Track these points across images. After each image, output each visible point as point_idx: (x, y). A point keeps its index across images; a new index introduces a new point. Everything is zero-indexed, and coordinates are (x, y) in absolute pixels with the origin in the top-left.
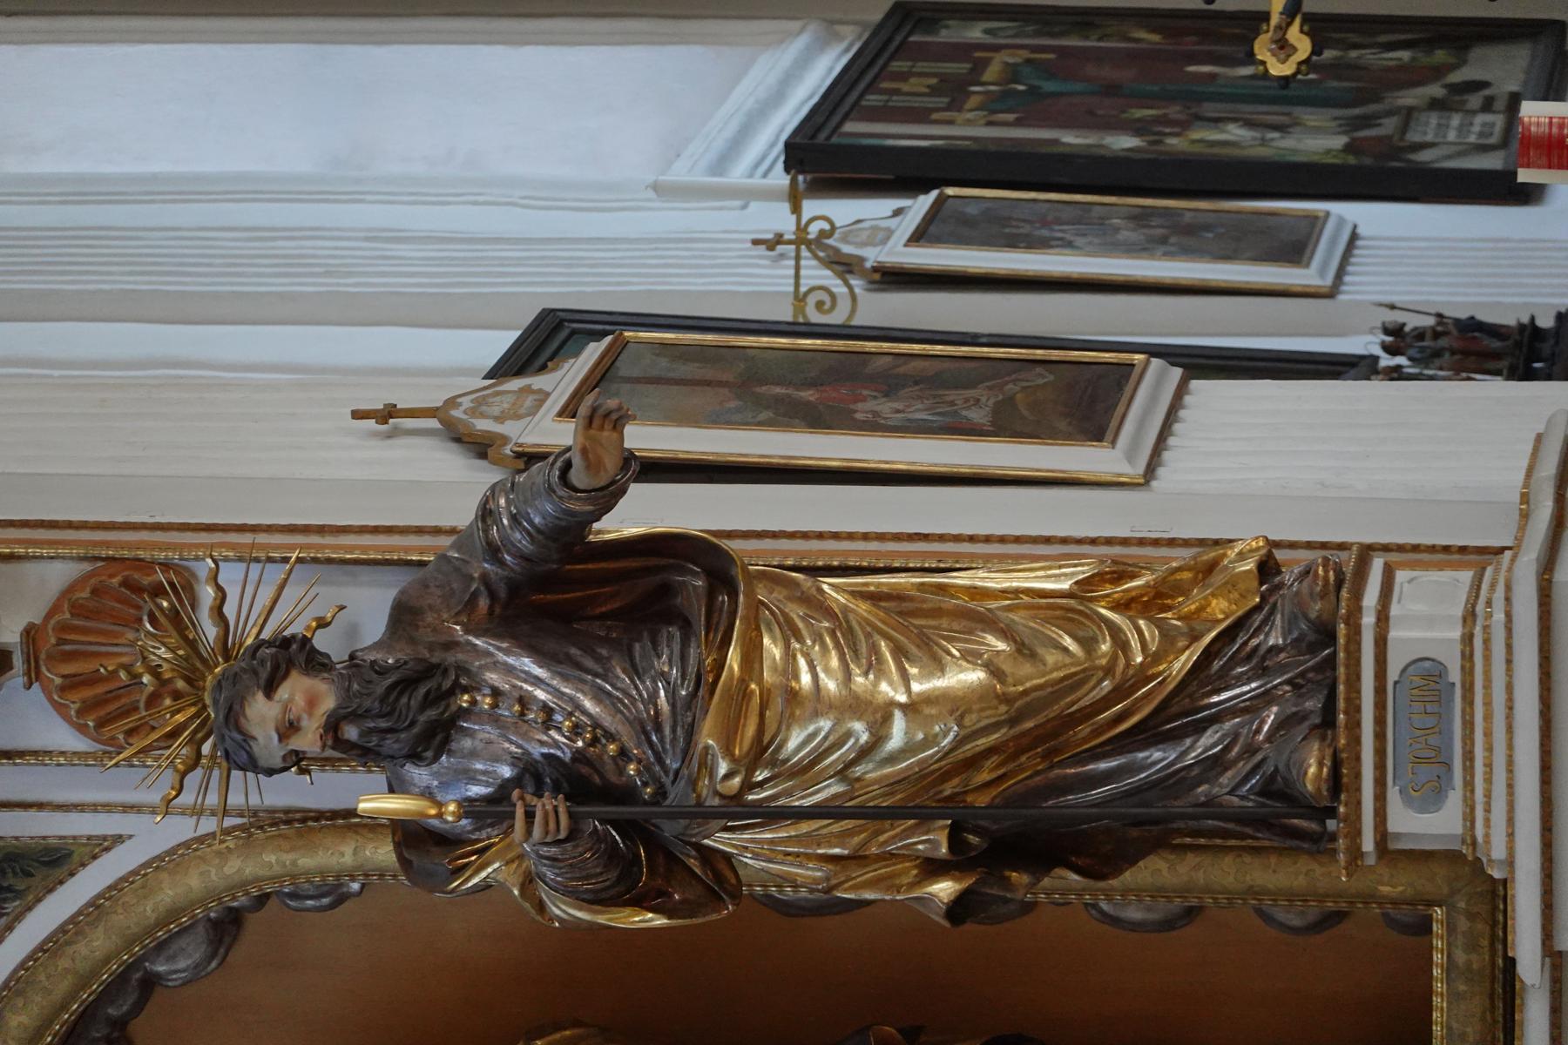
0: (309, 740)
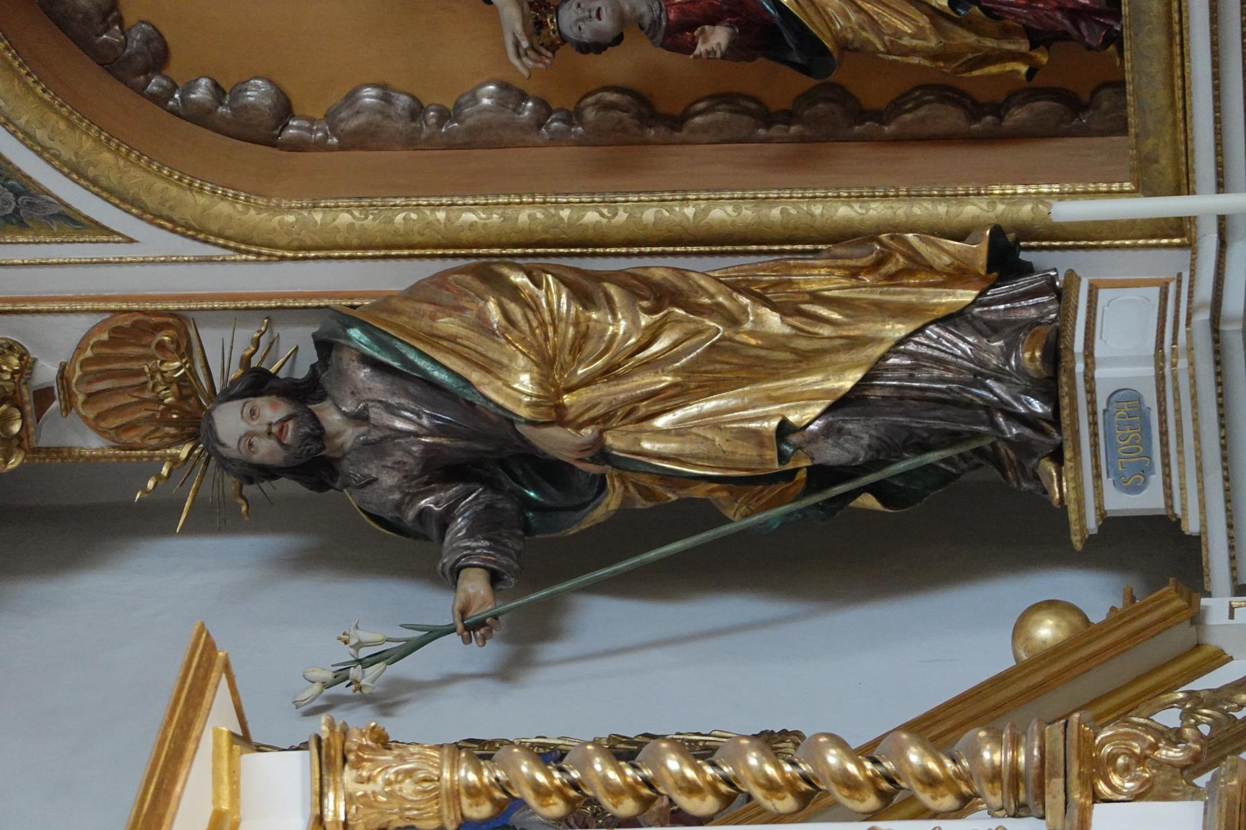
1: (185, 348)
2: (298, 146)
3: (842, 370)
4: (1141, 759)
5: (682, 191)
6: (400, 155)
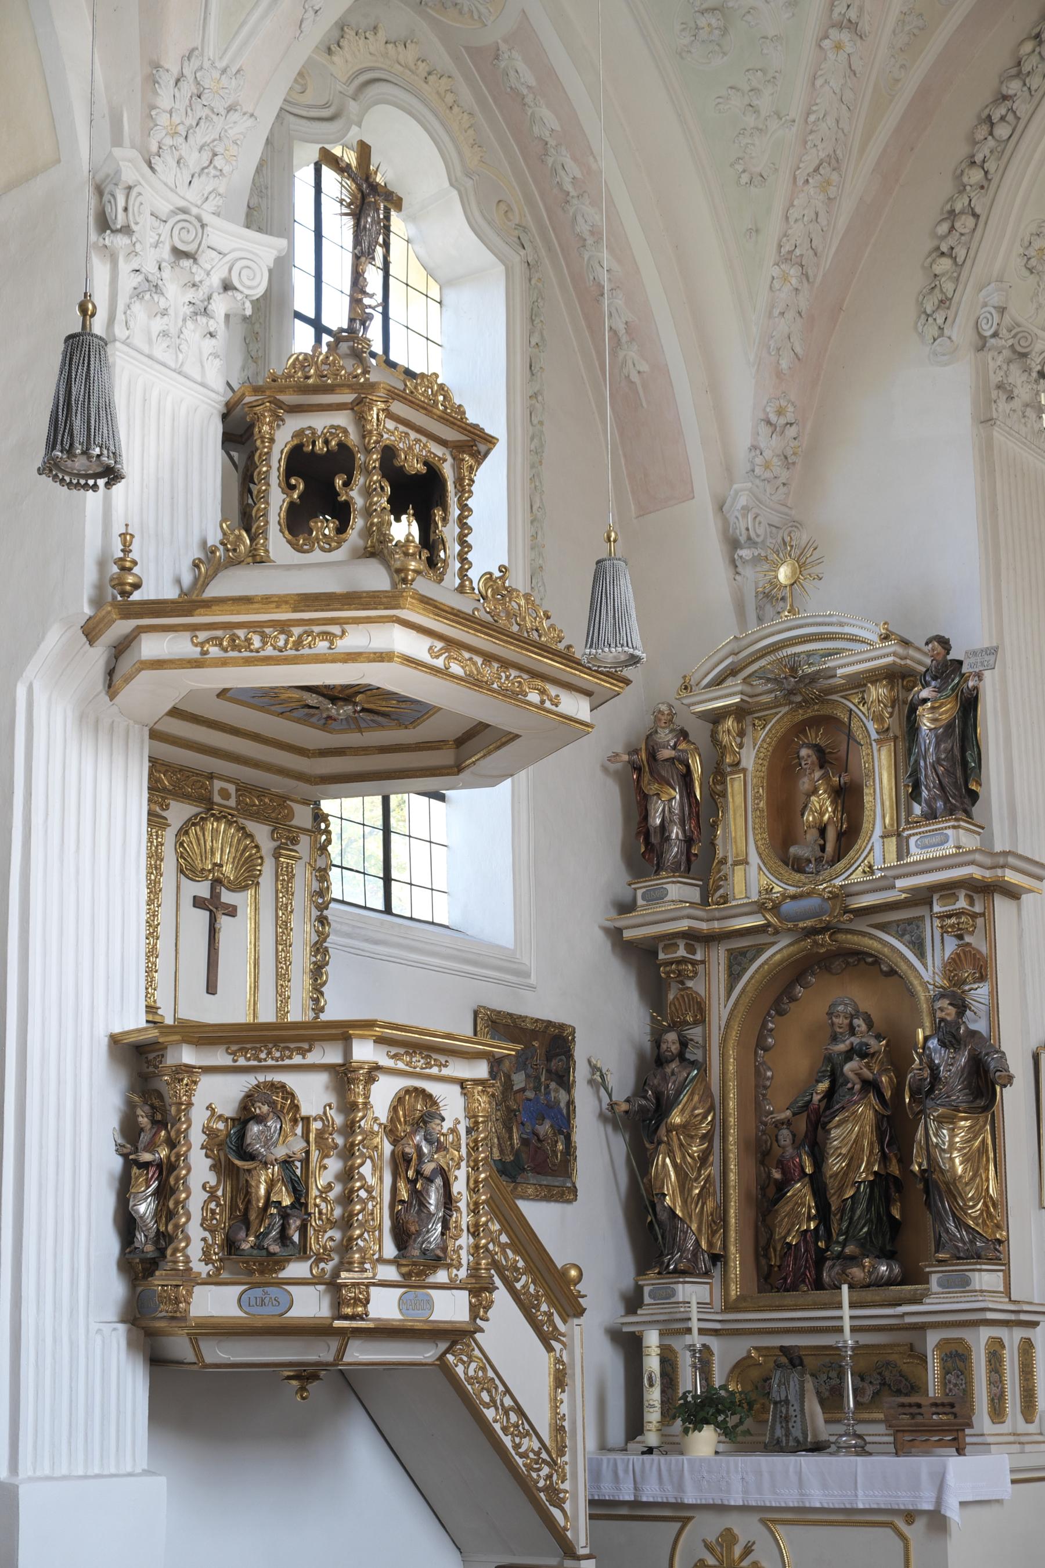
0: (939, 1014)
1: (696, 1023)
2: (756, 1053)
3: (682, 1211)
4: (481, 1304)
5: (738, 1165)
6: (753, 1083)
